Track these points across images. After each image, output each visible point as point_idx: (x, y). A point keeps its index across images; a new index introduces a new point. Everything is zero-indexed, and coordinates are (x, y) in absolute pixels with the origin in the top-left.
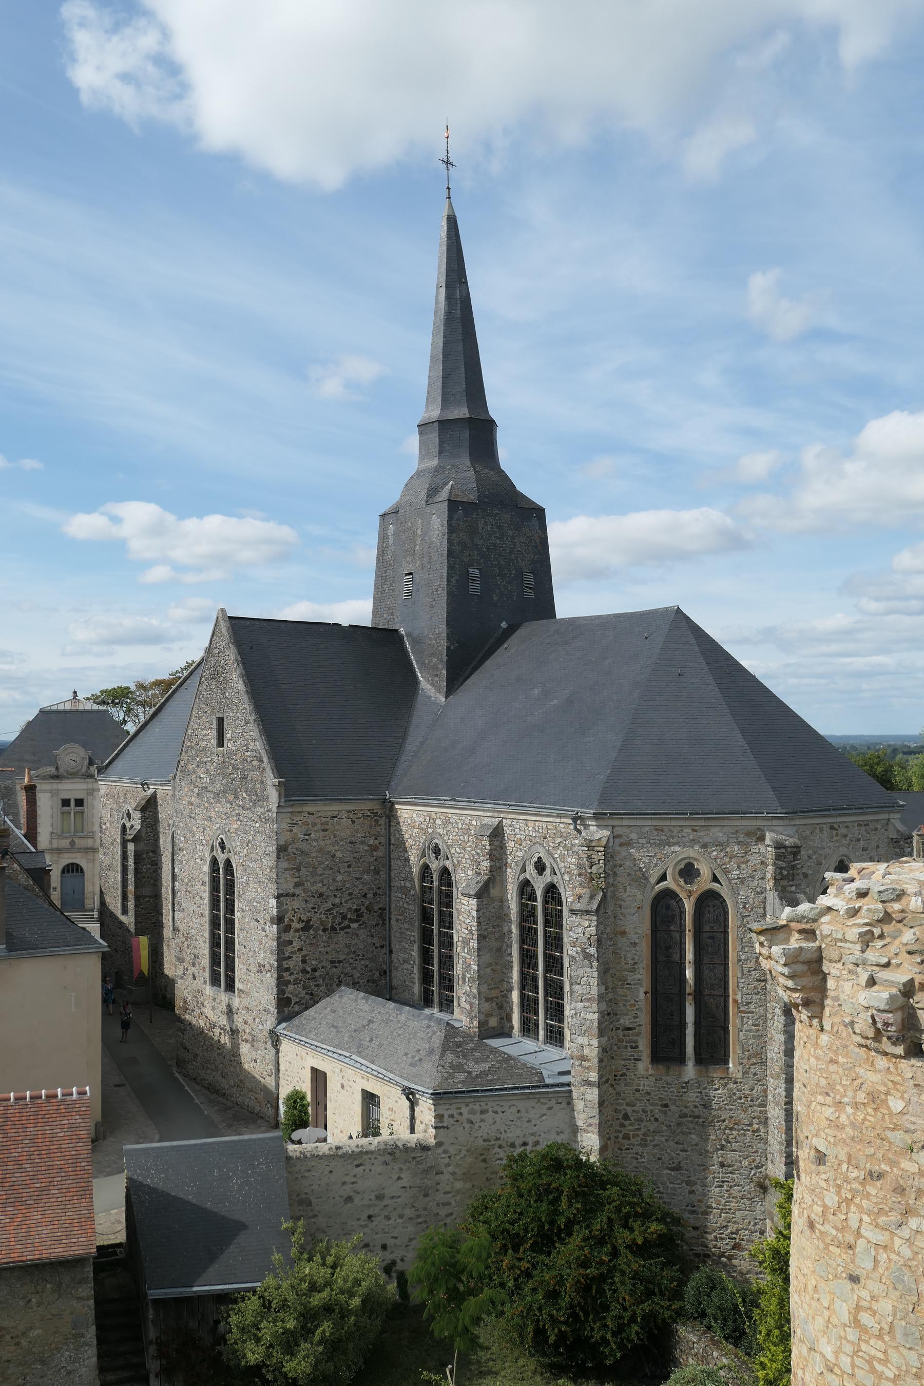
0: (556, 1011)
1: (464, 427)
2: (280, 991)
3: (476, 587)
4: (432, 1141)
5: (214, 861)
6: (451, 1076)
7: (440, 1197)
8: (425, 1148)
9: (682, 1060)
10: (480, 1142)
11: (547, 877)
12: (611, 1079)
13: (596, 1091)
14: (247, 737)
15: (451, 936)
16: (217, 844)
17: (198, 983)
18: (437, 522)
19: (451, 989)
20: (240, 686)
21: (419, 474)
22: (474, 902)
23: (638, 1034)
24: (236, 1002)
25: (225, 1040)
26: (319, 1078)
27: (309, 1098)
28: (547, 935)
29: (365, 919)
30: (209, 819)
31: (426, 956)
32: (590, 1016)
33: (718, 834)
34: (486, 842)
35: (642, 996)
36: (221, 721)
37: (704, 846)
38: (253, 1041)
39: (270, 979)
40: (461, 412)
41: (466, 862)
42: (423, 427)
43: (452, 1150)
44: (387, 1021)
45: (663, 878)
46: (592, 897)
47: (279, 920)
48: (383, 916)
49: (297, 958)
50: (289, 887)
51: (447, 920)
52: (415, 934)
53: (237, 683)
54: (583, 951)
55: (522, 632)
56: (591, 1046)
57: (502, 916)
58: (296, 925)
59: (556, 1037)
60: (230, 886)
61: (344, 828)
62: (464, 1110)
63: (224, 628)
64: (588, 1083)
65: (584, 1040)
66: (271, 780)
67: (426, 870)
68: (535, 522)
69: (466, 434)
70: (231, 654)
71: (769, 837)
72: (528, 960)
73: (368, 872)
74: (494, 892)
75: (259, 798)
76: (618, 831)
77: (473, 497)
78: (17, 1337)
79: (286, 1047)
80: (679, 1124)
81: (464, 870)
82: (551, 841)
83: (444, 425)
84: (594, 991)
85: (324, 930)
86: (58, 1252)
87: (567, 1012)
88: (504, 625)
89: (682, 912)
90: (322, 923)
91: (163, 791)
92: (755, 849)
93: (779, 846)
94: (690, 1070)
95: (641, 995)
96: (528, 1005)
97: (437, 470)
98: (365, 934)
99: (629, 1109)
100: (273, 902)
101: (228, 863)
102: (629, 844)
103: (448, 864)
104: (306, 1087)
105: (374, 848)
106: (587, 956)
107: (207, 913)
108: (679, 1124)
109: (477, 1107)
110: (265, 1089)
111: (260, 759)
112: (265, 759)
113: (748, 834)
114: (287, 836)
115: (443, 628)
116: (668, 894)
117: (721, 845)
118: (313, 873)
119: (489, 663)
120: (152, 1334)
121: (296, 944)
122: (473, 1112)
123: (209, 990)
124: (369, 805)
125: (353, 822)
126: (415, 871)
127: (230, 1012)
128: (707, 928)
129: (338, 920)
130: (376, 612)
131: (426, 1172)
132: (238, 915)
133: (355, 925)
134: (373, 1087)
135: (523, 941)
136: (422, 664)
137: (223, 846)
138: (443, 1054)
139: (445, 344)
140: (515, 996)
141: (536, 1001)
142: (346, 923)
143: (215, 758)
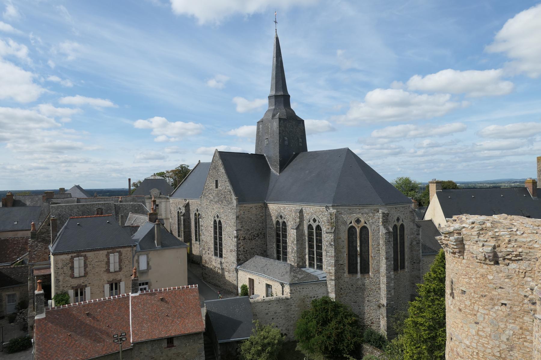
0: (320, 260)
1: (281, 97)
2: (238, 257)
3: (286, 143)
4: (289, 297)
5: (215, 221)
6: (294, 279)
7: (292, 312)
8: (288, 299)
9: (357, 273)
10: (302, 297)
11: (317, 223)
12: (338, 278)
13: (334, 282)
14: (225, 185)
15: (286, 240)
16: (216, 216)
17: (210, 255)
18: (275, 124)
19: (286, 255)
20: (223, 171)
21: (269, 110)
22: (295, 231)
24: (223, 260)
25: (220, 271)
26: (251, 281)
27: (248, 287)
28: (317, 239)
30: (213, 209)
31: (278, 246)
32: (332, 261)
33: (366, 210)
34: (298, 214)
36: (217, 181)
37: (362, 214)
38: (229, 271)
39: (235, 254)
40: (281, 93)
41: (291, 219)
42: (270, 97)
43: (295, 299)
44: (272, 264)
45: (351, 223)
46: (332, 229)
47: (237, 237)
48: (265, 235)
49: (242, 247)
50: (239, 228)
51: (285, 236)
52: (275, 240)
53: (222, 170)
54: (330, 243)
55: (300, 155)
56: (332, 270)
57: (303, 235)
58: (241, 238)
59: (320, 267)
60: (221, 228)
61: (254, 211)
62: (298, 288)
63: (217, 154)
64: (332, 280)
65: (330, 268)
66: (234, 197)
67: (278, 222)
68: (301, 124)
69: (283, 99)
70: (220, 162)
71: (380, 211)
72: (311, 246)
73: (260, 223)
74: (300, 228)
75: (230, 203)
76: (338, 210)
77: (285, 117)
79: (240, 273)
81: (290, 222)
82: (319, 213)
83: (276, 97)
84: (333, 254)
86: (194, 331)
87: (323, 260)
88: (294, 153)
89: (356, 232)
91: (191, 201)
92: (376, 214)
93: (383, 213)
94: (359, 275)
95: (345, 255)
96: (311, 259)
97: (274, 109)
98: (262, 241)
99: (342, 287)
100: (235, 232)
101: (220, 221)
102: (341, 214)
103: (285, 220)
104: (247, 284)
105: (262, 216)
106: (331, 245)
107: (213, 235)
109: (301, 287)
110: (233, 285)
111: (230, 192)
112: (232, 192)
113: (374, 210)
114: (239, 213)
115: (278, 154)
116: (352, 227)
117: (367, 214)
118: (246, 224)
119: (291, 164)
120: (219, 353)
121: (242, 244)
122: (300, 289)
123: (214, 257)
124: (260, 204)
126: (274, 222)
127: (221, 263)
128: (363, 236)
130: (256, 150)
131: (288, 305)
132: (223, 236)
134: (269, 283)
135: (309, 241)
136: (271, 165)
137: (218, 217)
138: (290, 273)
139: (276, 74)
140: (307, 257)
141: (313, 258)
143: (215, 192)
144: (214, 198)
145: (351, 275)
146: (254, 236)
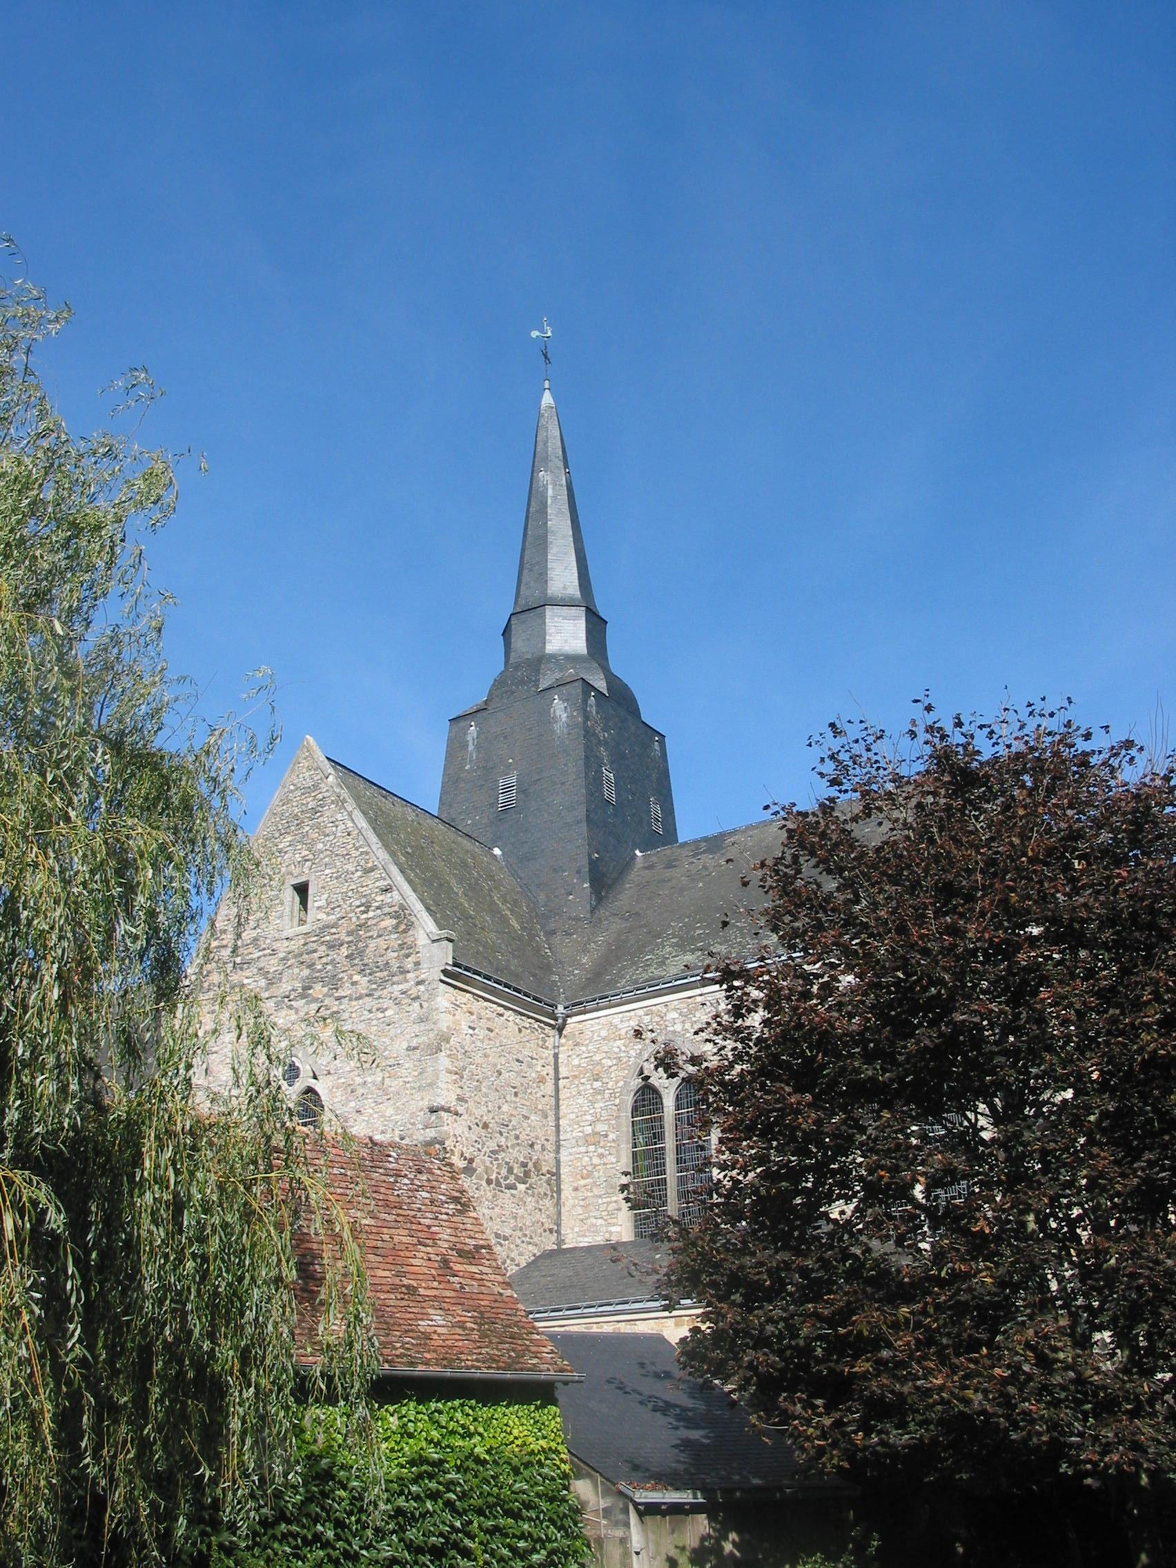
29: (534, 1179)
36: (302, 890)
85: (489, 1182)
90: (487, 1170)
125: (520, 1031)
129: (504, 1172)
133: (522, 1187)
142: (512, 1180)
146: (510, 1170)
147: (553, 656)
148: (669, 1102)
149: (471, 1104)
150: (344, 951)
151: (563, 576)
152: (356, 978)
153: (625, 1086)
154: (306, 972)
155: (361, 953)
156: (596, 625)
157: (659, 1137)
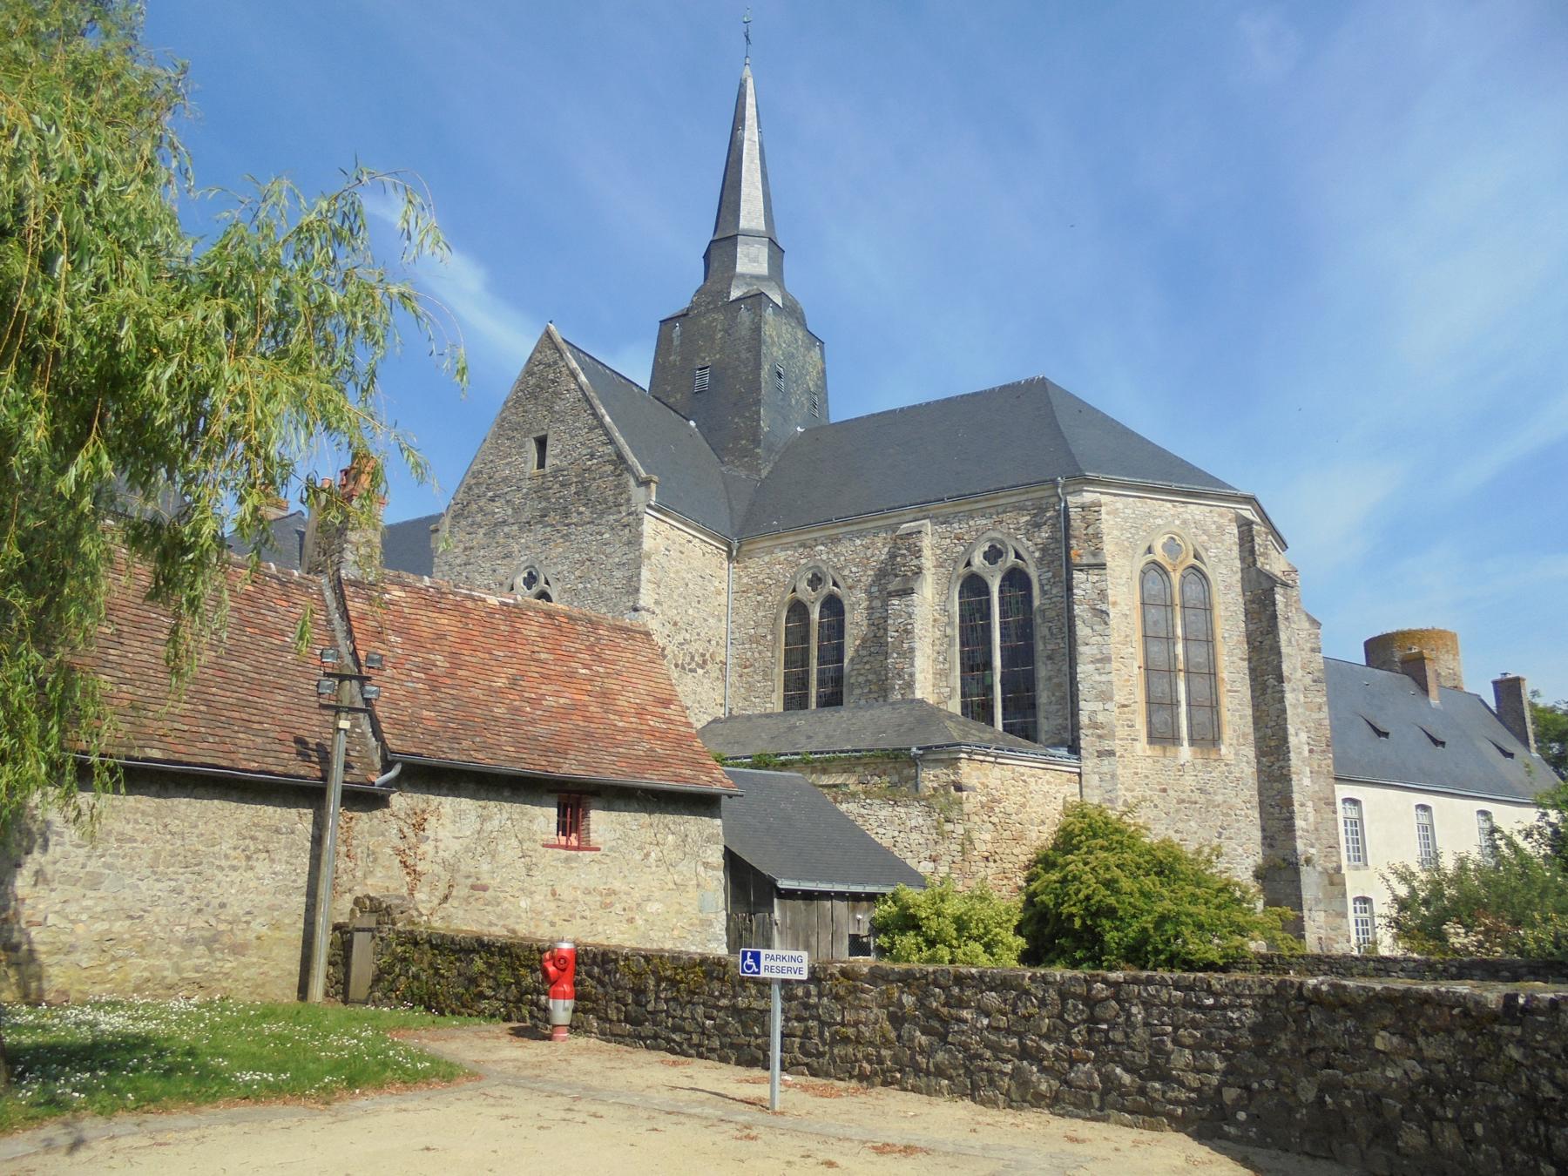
23: (1134, 712)
35: (1136, 671)
36: (542, 443)
78: (631, 909)
80: (1177, 811)
85: (676, 666)
108: (1177, 811)
129: (688, 659)
133: (700, 671)
142: (693, 666)
144: (517, 511)
145: (1158, 750)
146: (692, 658)
147: (743, 276)
148: (815, 615)
149: (665, 606)
150: (573, 489)
151: (751, 214)
152: (582, 509)
153: (779, 599)
154: (544, 504)
155: (586, 489)
156: (776, 252)
157: (805, 638)
